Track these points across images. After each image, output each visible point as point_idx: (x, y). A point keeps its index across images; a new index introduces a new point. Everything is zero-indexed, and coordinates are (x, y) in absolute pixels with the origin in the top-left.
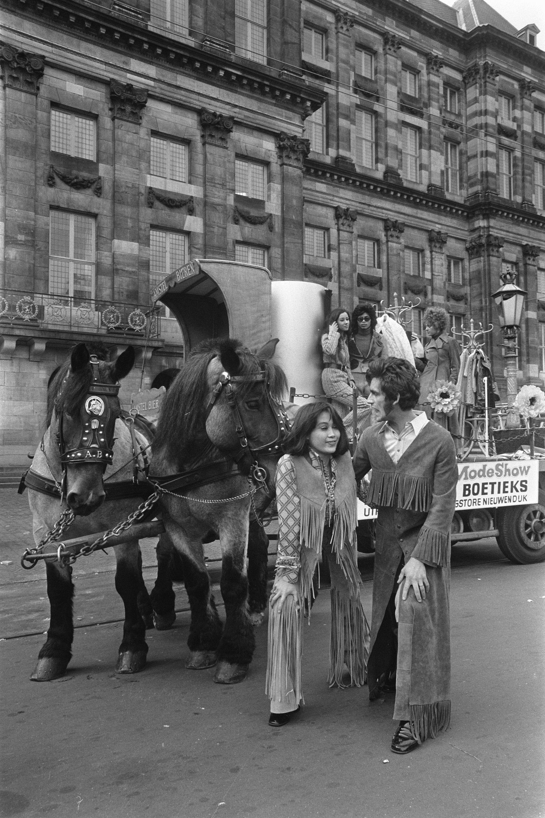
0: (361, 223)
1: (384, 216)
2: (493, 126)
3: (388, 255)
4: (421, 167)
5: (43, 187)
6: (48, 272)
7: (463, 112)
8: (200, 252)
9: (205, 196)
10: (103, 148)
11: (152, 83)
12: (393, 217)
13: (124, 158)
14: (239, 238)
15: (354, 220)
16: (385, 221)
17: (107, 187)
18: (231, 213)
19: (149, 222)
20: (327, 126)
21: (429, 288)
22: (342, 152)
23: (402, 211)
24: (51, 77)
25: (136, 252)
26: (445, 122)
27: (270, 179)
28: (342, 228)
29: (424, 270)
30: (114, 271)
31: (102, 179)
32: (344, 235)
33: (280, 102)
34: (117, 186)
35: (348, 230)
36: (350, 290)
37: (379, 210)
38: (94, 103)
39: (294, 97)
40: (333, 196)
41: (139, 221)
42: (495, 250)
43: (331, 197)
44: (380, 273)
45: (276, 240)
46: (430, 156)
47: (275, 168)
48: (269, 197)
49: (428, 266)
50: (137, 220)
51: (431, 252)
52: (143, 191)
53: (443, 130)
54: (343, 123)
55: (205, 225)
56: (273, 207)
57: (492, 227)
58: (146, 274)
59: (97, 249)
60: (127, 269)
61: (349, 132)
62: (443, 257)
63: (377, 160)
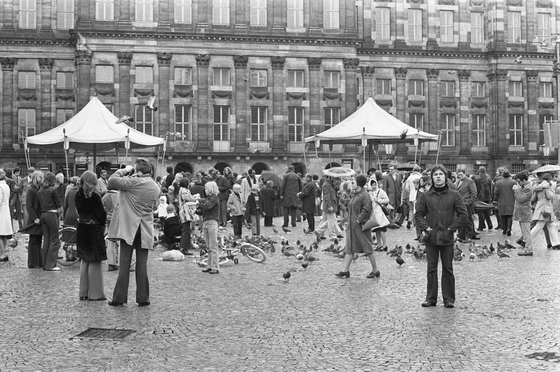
0: (411, 74)
1: (426, 67)
4: (455, 33)
11: (287, 52)
12: (431, 66)
13: (277, 84)
15: (405, 73)
16: (427, 69)
20: (390, 24)
21: (458, 102)
22: (399, 38)
24: (251, 60)
30: (274, 127)
33: (344, 45)
36: (404, 110)
38: (266, 65)
39: (349, 43)
42: (501, 77)
44: (423, 98)
45: (343, 104)
49: (458, 90)
54: (399, 21)
55: (310, 104)
57: (500, 64)
61: (403, 26)
63: (423, 36)
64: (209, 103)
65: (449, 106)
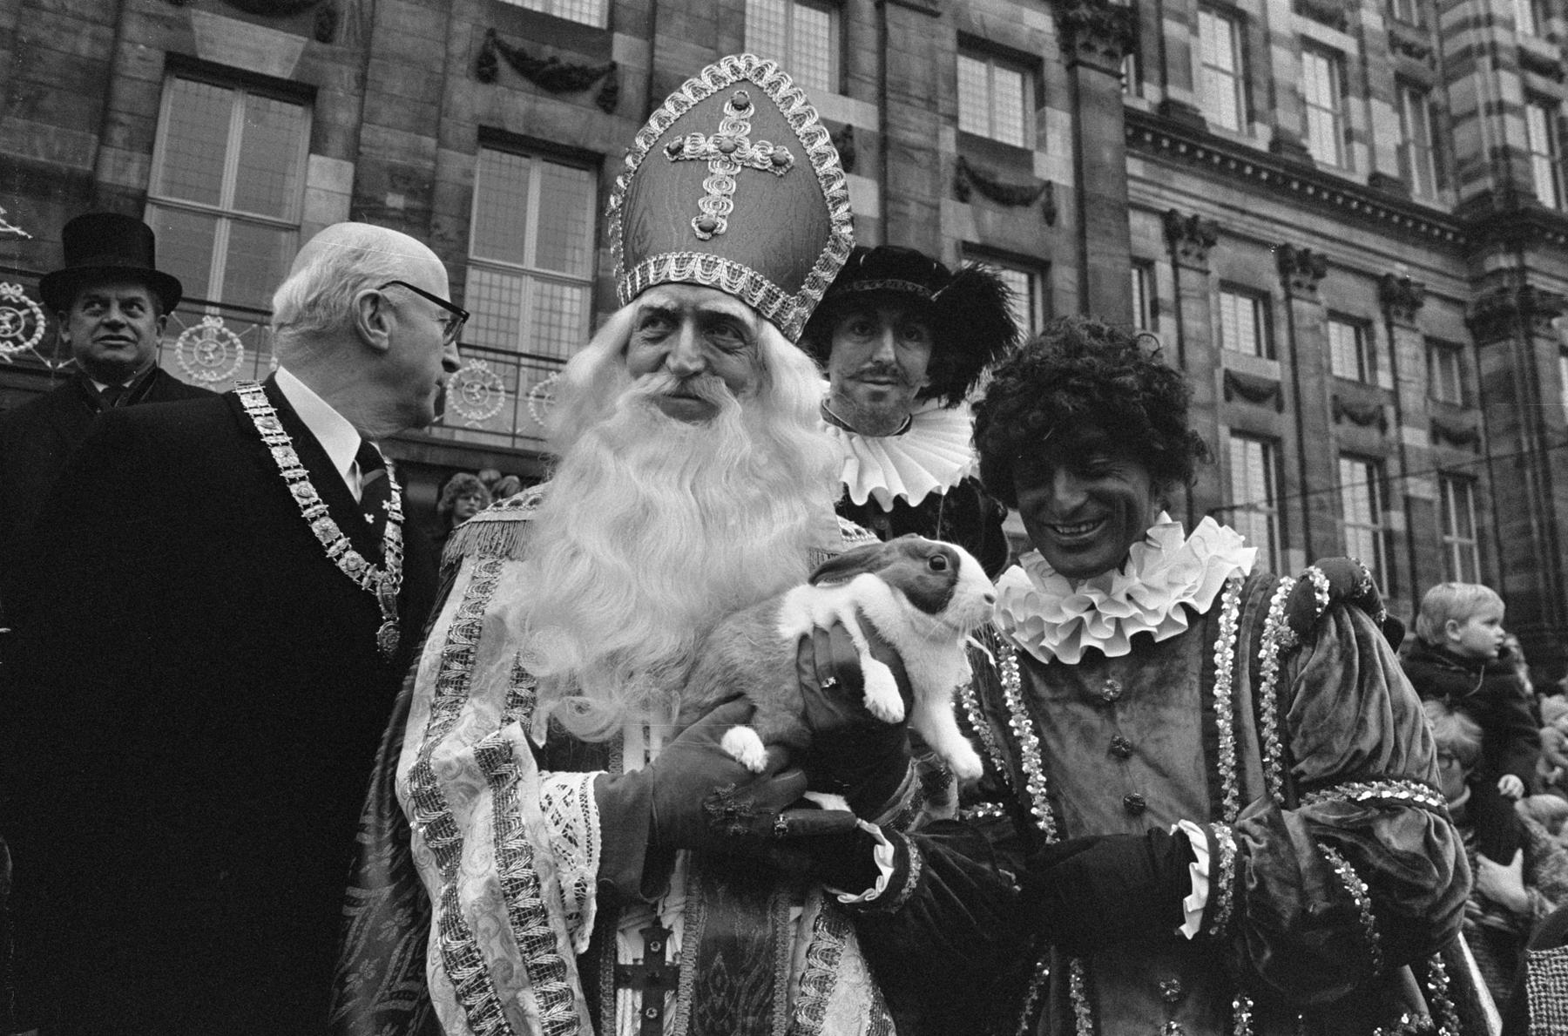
0: (1224, 256)
2: (1507, 49)
3: (1291, 328)
4: (1350, 136)
7: (1431, 23)
9: (884, 124)
12: (1299, 242)
13: (680, 22)
14: (972, 237)
16: (1283, 251)
18: (949, 173)
21: (1390, 412)
22: (1175, 93)
23: (1318, 229)
26: (1394, 43)
27: (1041, 98)
28: (1183, 260)
29: (1374, 368)
31: (620, 69)
32: (1189, 278)
34: (660, 86)
35: (1197, 265)
37: (1267, 224)
40: (1161, 186)
42: (1545, 321)
43: (1155, 190)
44: (1275, 371)
46: (1368, 112)
47: (1055, 72)
48: (1042, 143)
49: (1383, 359)
51: (1389, 326)
53: (1391, 58)
55: (885, 197)
56: (1054, 165)
57: (1534, 271)
61: (1187, 51)
62: (1418, 338)
63: (1252, 116)
64: (132, 28)
65: (1362, 420)
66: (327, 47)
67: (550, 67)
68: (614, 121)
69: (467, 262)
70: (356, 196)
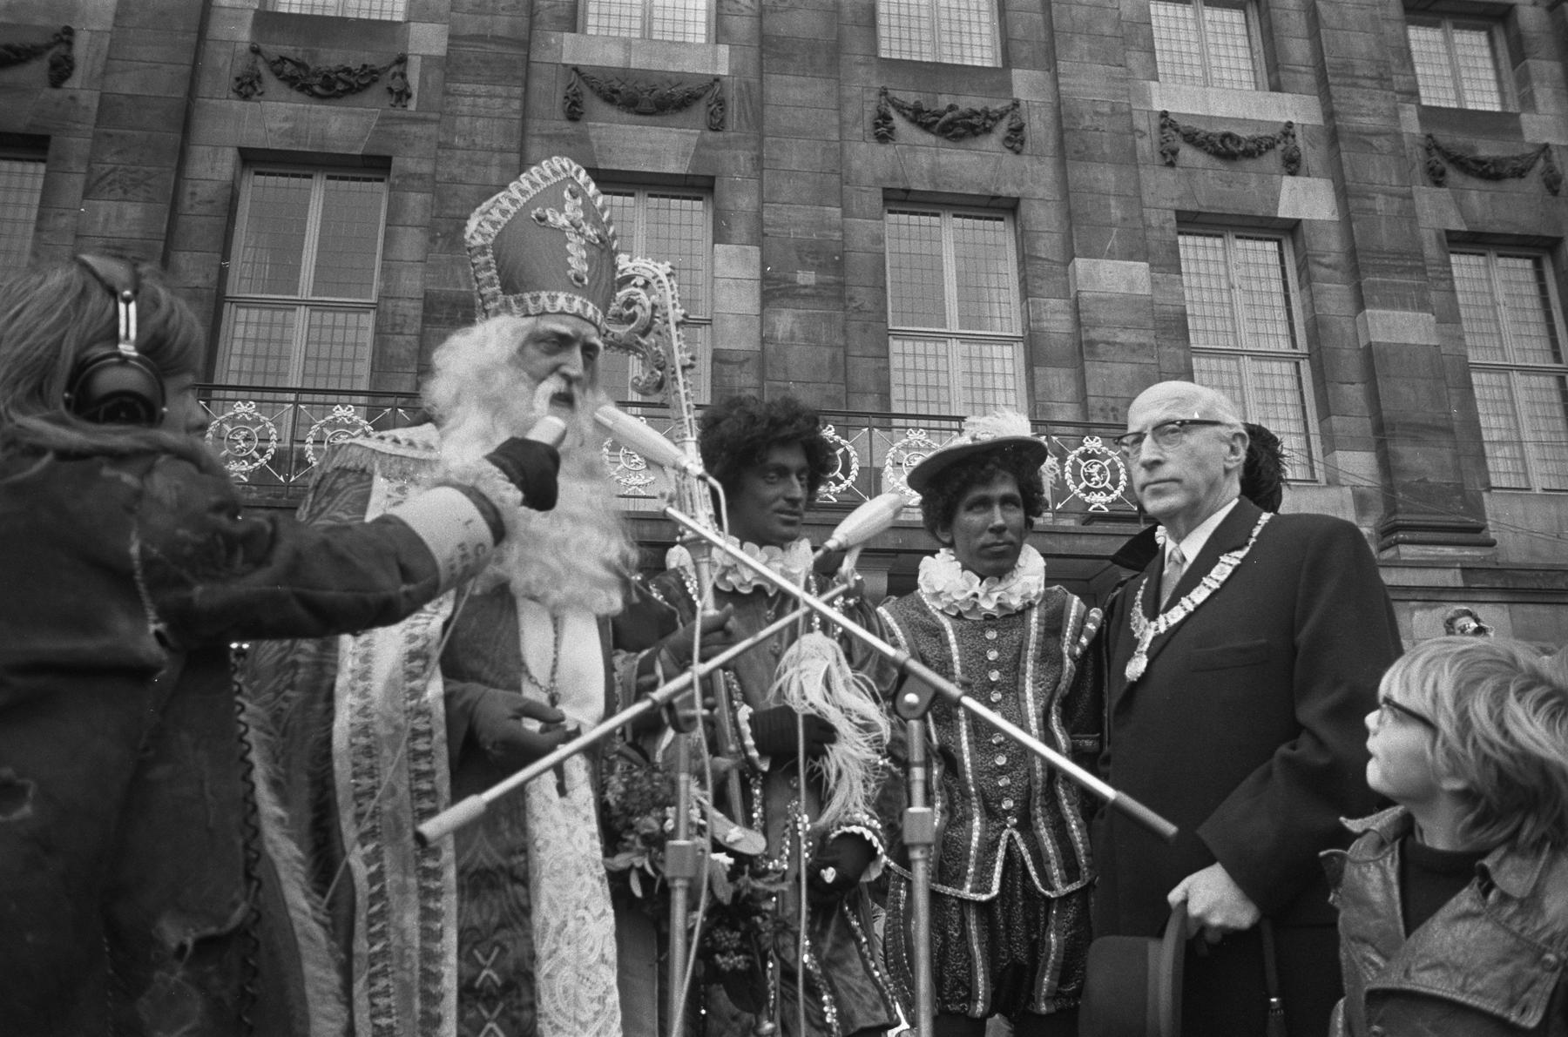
5: (863, 146)
6: (887, 368)
8: (1338, 274)
9: (1330, 115)
10: (1019, 31)
13: (1082, 44)
14: (1456, 224)
17: (1039, 126)
18: (1419, 154)
19: (1169, 204)
25: (1143, 289)
31: (1023, 105)
34: (1070, 115)
41: (1142, 205)
50: (1135, 199)
52: (1141, 124)
55: (1343, 194)
58: (1181, 352)
59: (1026, 292)
60: (1122, 337)
66: (720, 135)
67: (949, 115)
68: (1025, 161)
69: (888, 333)
70: (765, 278)
